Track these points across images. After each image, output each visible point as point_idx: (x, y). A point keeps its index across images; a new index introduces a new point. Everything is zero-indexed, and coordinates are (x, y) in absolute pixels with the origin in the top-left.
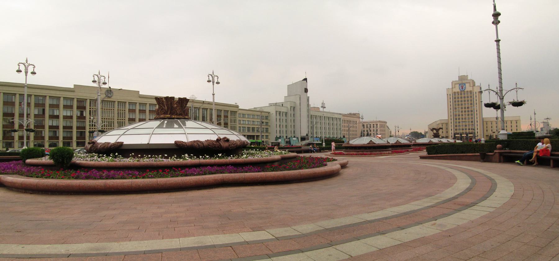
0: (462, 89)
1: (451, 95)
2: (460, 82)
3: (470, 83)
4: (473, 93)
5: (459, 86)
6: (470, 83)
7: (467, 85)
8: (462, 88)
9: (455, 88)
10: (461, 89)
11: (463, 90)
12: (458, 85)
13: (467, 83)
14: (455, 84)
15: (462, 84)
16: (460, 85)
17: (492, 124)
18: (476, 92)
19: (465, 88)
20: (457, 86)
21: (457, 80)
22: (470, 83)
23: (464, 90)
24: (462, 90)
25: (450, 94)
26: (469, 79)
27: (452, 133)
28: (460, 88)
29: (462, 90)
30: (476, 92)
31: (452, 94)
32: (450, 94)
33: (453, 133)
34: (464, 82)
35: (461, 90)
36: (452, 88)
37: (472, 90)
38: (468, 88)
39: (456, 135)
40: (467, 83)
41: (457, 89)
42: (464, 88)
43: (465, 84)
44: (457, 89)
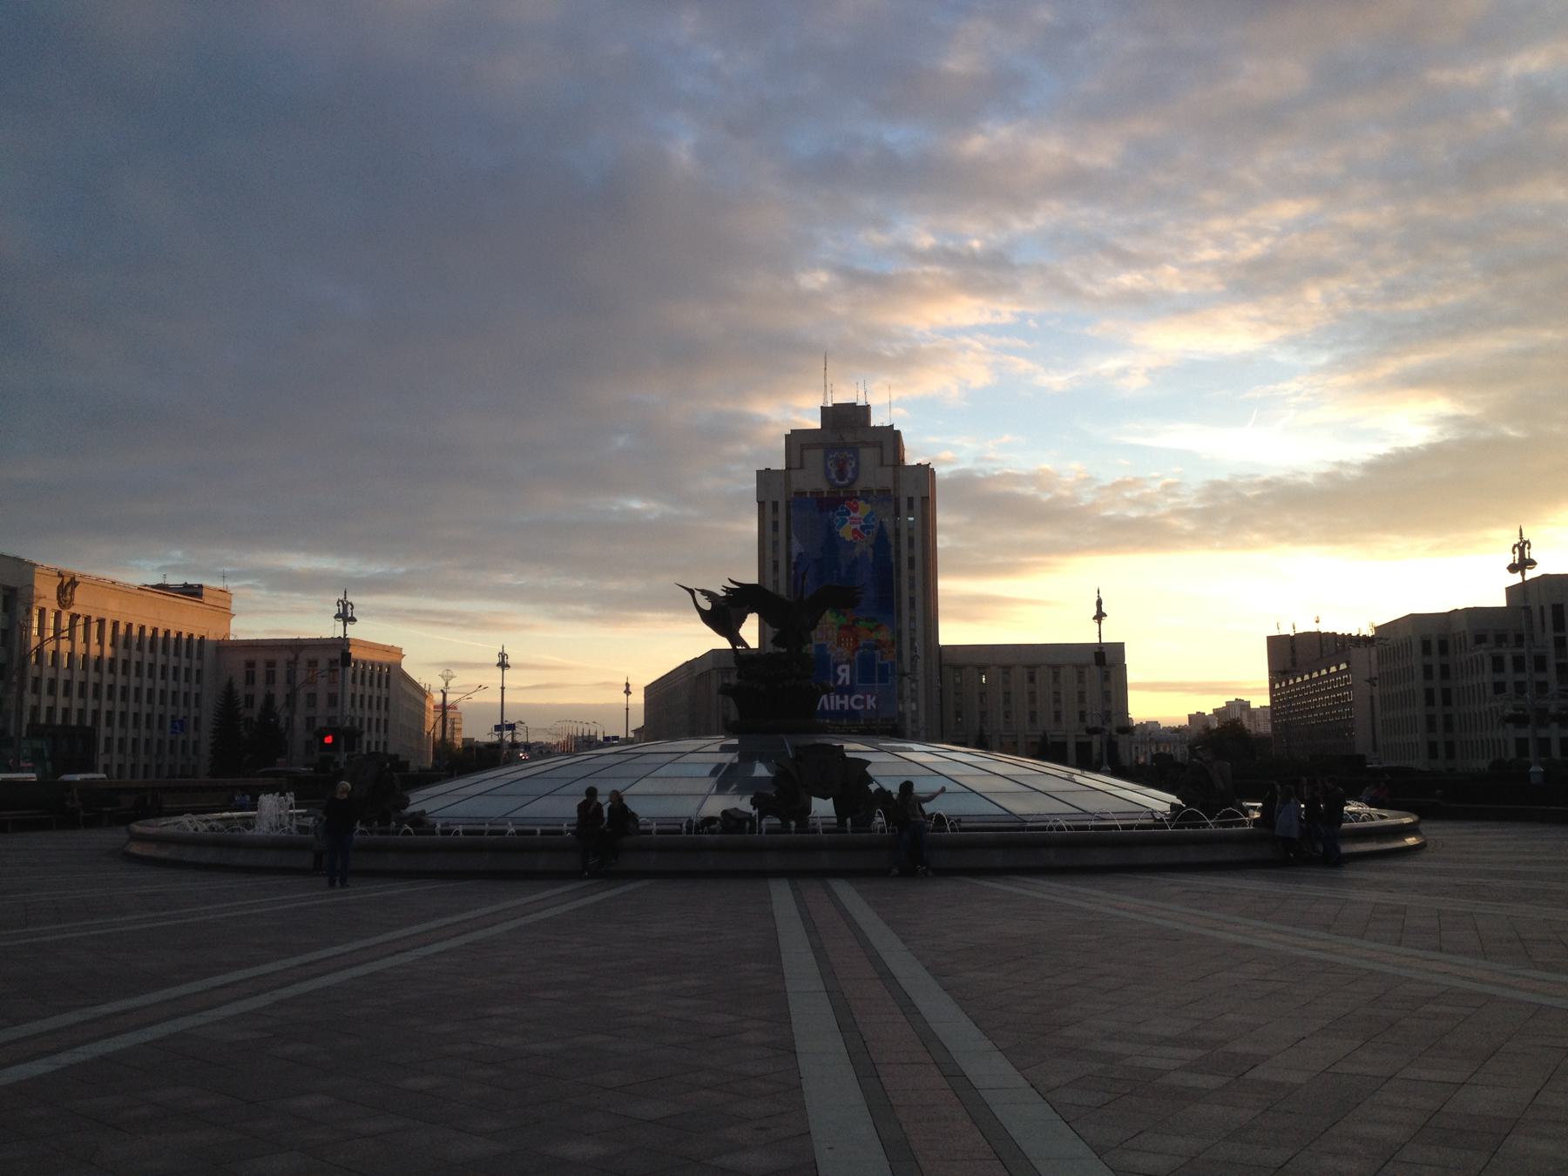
0: (841, 473)
6: (880, 445)
7: (868, 456)
8: (841, 473)
9: (802, 467)
10: (833, 476)
11: (847, 481)
12: (820, 453)
13: (866, 444)
14: (803, 448)
18: (910, 500)
19: (856, 471)
20: (814, 458)
21: (818, 425)
22: (881, 447)
23: (853, 481)
24: (837, 481)
25: (775, 505)
26: (877, 420)
28: (827, 473)
29: (837, 481)
30: (910, 500)
31: (788, 502)
32: (775, 505)
35: (831, 482)
37: (890, 485)
38: (872, 476)
41: (813, 480)
42: (850, 475)
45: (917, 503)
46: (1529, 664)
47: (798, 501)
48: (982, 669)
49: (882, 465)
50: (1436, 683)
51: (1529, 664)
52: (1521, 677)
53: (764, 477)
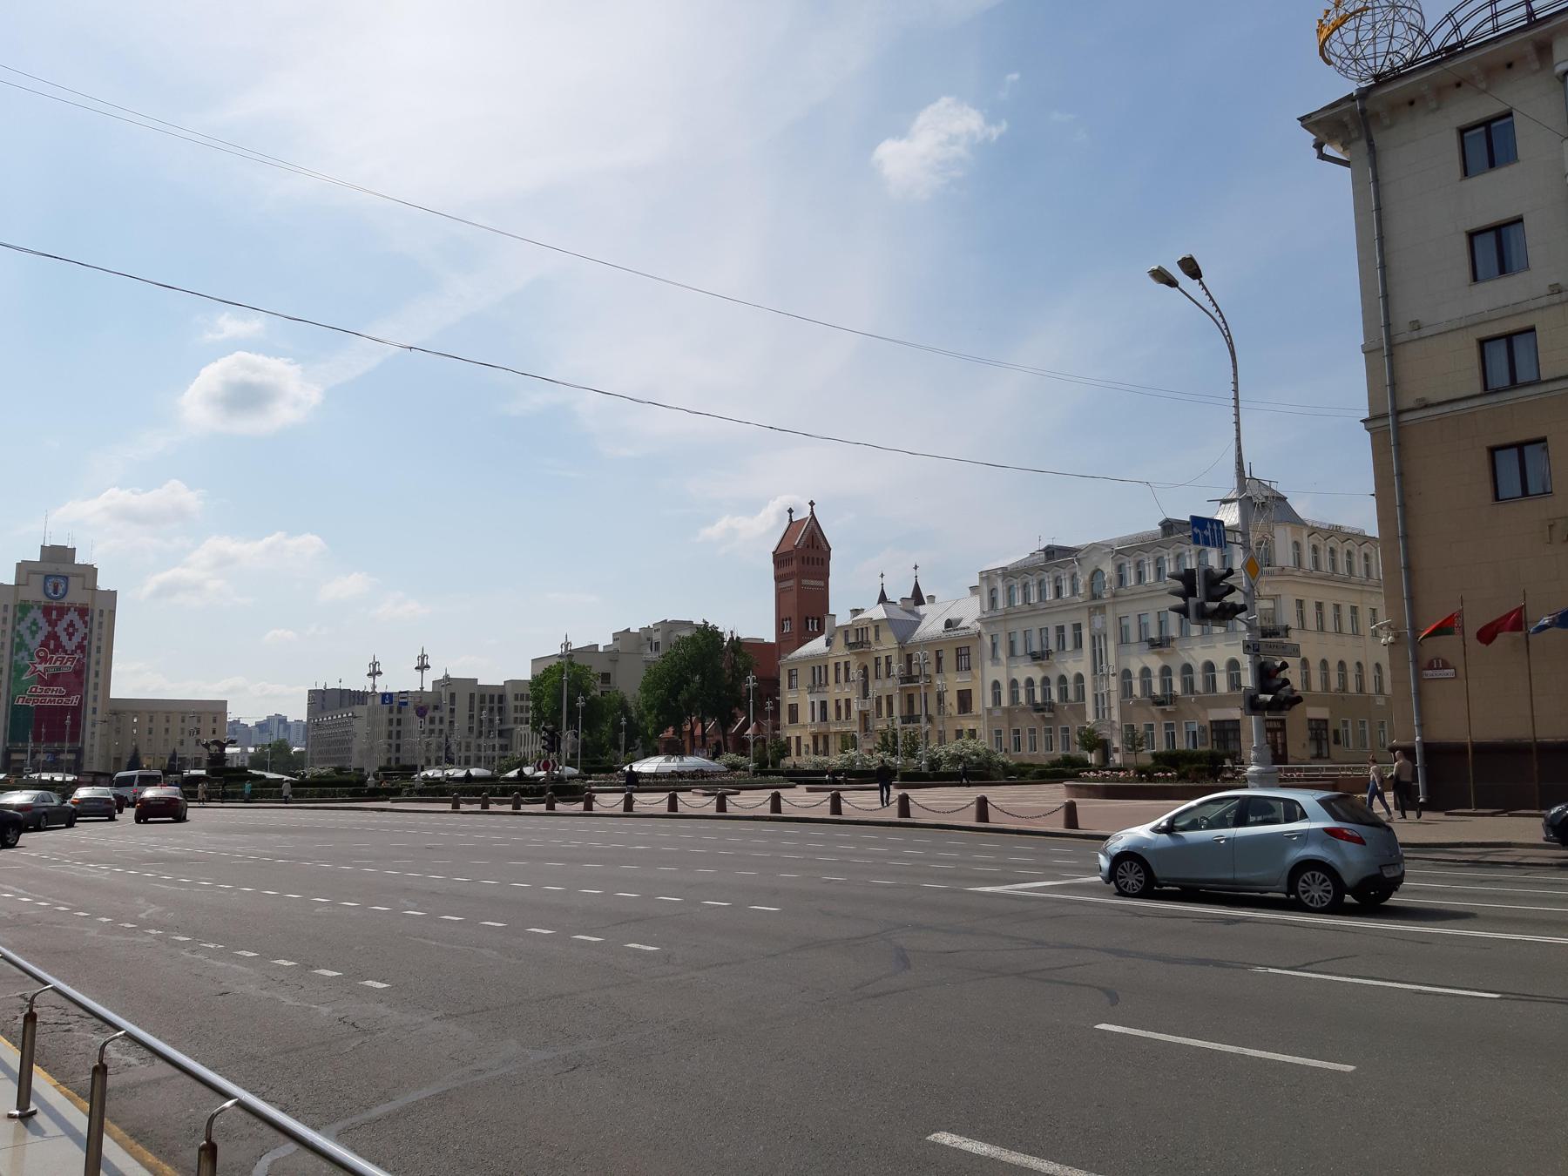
0: (56, 592)
1: (11, 609)
2: (51, 568)
3: (83, 576)
4: (92, 610)
5: (45, 584)
7: (74, 583)
8: (56, 592)
10: (50, 591)
12: (41, 578)
13: (77, 576)
15: (57, 576)
16: (47, 577)
18: (101, 611)
30: (101, 611)
31: (15, 606)
34: (64, 569)
35: (47, 595)
36: (17, 585)
40: (77, 576)
41: (35, 594)
42: (60, 591)
43: (66, 578)
48: (136, 713)
49: (84, 588)
50: (394, 728)
52: (432, 727)
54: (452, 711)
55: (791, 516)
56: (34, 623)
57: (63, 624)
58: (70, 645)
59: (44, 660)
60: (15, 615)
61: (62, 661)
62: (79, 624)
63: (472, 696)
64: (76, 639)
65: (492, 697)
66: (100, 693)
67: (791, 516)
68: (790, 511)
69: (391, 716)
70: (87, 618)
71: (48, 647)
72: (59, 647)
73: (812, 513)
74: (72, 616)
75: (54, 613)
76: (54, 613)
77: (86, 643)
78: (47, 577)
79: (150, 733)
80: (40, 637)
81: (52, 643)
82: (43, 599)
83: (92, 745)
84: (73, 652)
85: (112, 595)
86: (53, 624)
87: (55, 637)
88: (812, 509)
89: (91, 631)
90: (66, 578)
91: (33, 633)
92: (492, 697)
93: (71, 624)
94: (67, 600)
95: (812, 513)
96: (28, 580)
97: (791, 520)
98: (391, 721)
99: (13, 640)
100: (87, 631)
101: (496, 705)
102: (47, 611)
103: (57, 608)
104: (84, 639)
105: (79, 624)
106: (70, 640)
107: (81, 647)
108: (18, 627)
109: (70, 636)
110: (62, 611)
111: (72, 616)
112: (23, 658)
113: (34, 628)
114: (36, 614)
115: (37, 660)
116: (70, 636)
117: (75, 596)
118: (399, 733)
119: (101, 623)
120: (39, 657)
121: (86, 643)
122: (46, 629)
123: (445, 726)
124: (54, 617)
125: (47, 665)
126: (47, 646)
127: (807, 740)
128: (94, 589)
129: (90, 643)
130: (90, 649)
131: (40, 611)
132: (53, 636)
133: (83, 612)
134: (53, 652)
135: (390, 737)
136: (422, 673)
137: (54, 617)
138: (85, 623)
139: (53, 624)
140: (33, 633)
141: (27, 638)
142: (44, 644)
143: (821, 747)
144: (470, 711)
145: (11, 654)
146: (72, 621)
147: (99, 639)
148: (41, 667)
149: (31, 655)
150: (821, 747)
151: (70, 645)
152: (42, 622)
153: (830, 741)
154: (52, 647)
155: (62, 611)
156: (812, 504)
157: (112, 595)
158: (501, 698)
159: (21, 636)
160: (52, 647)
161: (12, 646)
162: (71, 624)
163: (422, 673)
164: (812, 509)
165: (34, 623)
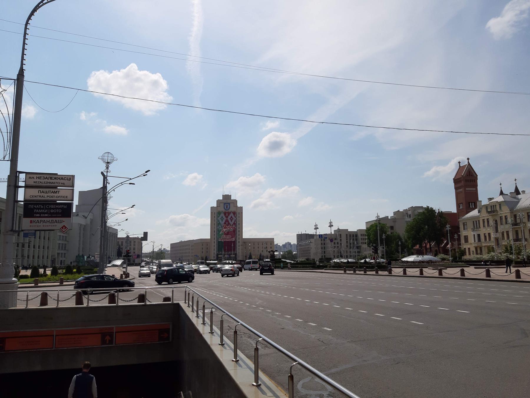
1: (216, 214)
2: (225, 201)
3: (234, 203)
4: (237, 213)
5: (224, 205)
7: (232, 205)
10: (226, 208)
12: (223, 204)
16: (225, 204)
17: (254, 245)
18: (239, 213)
23: (229, 209)
25: (215, 213)
27: (214, 253)
28: (224, 207)
30: (239, 213)
31: (217, 213)
33: (215, 253)
34: (229, 201)
35: (225, 209)
36: (217, 206)
39: (219, 256)
41: (222, 209)
42: (228, 208)
43: (229, 204)
44: (222, 209)
45: (240, 213)
46: (336, 243)
47: (219, 213)
48: (250, 243)
49: (234, 207)
51: (336, 243)
52: (335, 245)
53: (212, 208)
54: (341, 240)
55: (460, 165)
56: (222, 217)
57: (229, 217)
58: (232, 223)
59: (225, 228)
60: (217, 216)
61: (230, 228)
62: (233, 217)
63: (347, 235)
64: (233, 221)
65: (353, 235)
66: (240, 237)
67: (460, 165)
68: (459, 163)
69: (322, 242)
70: (236, 215)
71: (226, 224)
72: (229, 224)
73: (468, 162)
74: (232, 215)
75: (227, 214)
76: (227, 214)
77: (236, 222)
78: (225, 204)
79: (254, 248)
80: (224, 221)
81: (227, 223)
82: (224, 210)
83: (239, 252)
84: (233, 225)
85: (241, 208)
86: (227, 217)
87: (228, 221)
88: (468, 161)
89: (237, 219)
90: (229, 204)
91: (222, 220)
92: (353, 235)
93: (231, 217)
94: (230, 210)
95: (468, 162)
96: (220, 205)
97: (460, 166)
98: (322, 243)
99: (217, 222)
100: (236, 219)
101: (355, 238)
102: (225, 214)
103: (228, 213)
104: (235, 221)
105: (233, 217)
106: (231, 221)
107: (234, 224)
108: (218, 219)
109: (231, 220)
110: (229, 213)
111: (232, 215)
112: (220, 227)
113: (222, 219)
114: (222, 215)
115: (223, 228)
116: (231, 220)
117: (232, 209)
118: (324, 247)
119: (239, 216)
120: (224, 227)
121: (236, 222)
122: (225, 218)
123: (339, 245)
124: (227, 215)
125: (226, 229)
126: (226, 224)
127: (473, 249)
128: (237, 206)
129: (237, 222)
130: (237, 224)
131: (223, 214)
132: (227, 221)
133: (234, 213)
134: (228, 225)
135: (322, 249)
136: (331, 228)
137: (227, 215)
138: (235, 216)
139: (227, 217)
140: (222, 220)
141: (221, 221)
142: (225, 223)
143: (479, 251)
144: (346, 240)
145: (217, 226)
146: (232, 216)
147: (239, 221)
148: (224, 230)
149: (222, 226)
150: (479, 251)
151: (232, 223)
152: (224, 217)
153: (482, 249)
154: (227, 224)
155: (229, 213)
156: (468, 159)
157: (241, 208)
158: (356, 236)
159: (219, 221)
160: (227, 224)
161: (217, 224)
162: (231, 217)
163: (331, 228)
164: (468, 161)
165: (222, 217)
